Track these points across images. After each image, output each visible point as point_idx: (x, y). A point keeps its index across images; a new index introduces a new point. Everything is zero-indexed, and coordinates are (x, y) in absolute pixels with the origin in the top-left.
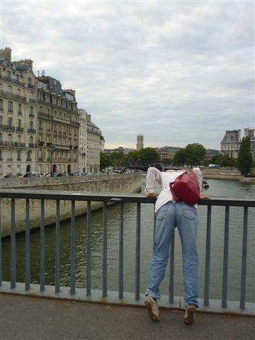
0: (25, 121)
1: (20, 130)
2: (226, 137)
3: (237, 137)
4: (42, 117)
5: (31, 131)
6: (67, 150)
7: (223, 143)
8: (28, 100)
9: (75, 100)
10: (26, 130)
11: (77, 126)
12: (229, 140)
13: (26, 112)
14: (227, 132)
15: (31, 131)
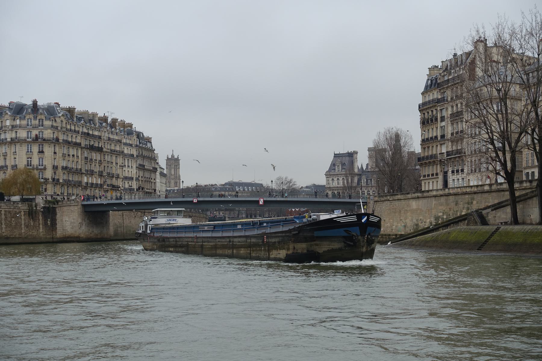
0: (134, 171)
1: (132, 179)
2: (333, 165)
3: (352, 163)
4: (141, 167)
5: (137, 179)
6: (151, 193)
7: (328, 175)
8: (135, 156)
9: (152, 147)
10: (134, 178)
11: (155, 170)
12: (338, 169)
13: (134, 167)
14: (336, 156)
15: (137, 179)
